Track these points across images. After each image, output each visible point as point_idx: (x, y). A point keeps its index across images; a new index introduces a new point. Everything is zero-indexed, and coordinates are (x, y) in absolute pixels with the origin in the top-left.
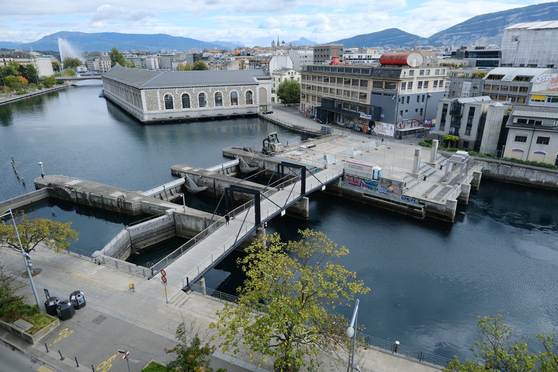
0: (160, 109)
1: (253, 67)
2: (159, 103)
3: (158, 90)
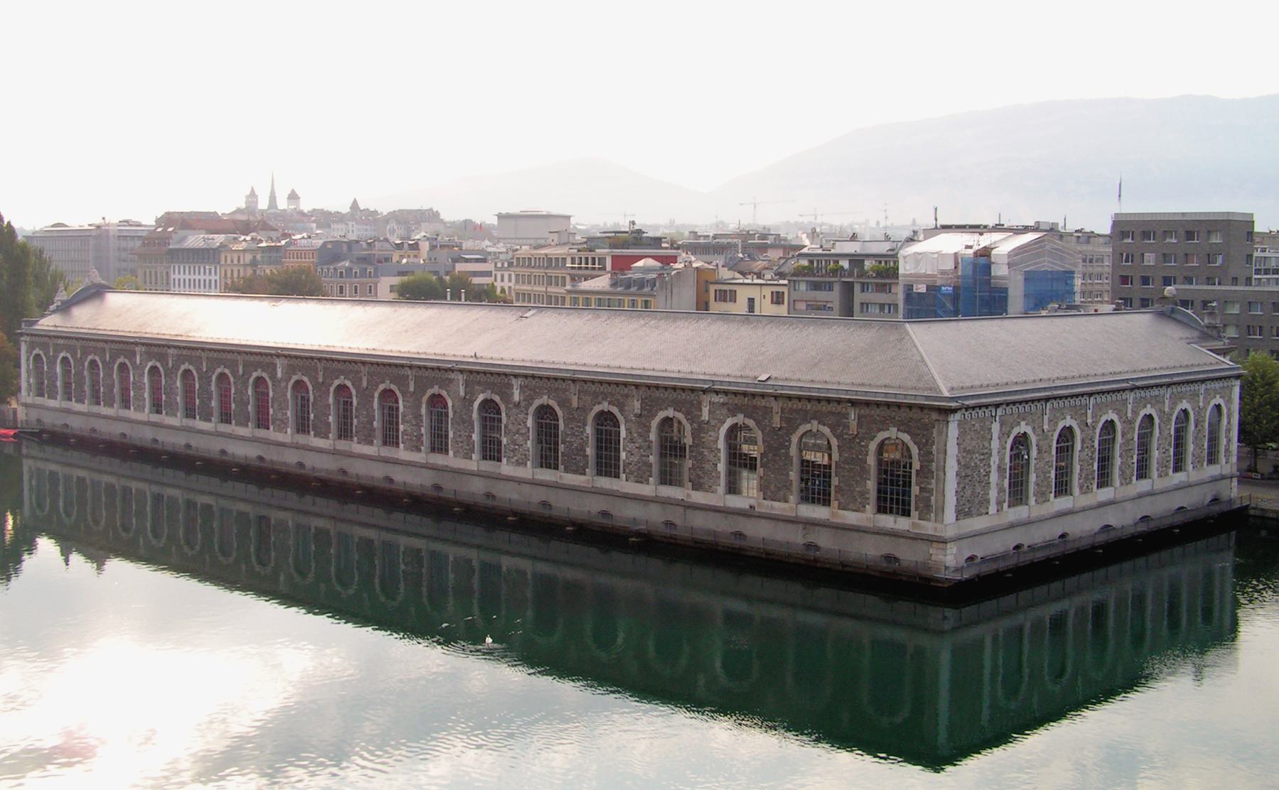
0: (992, 509)
1: (833, 297)
2: (994, 477)
3: (1000, 411)
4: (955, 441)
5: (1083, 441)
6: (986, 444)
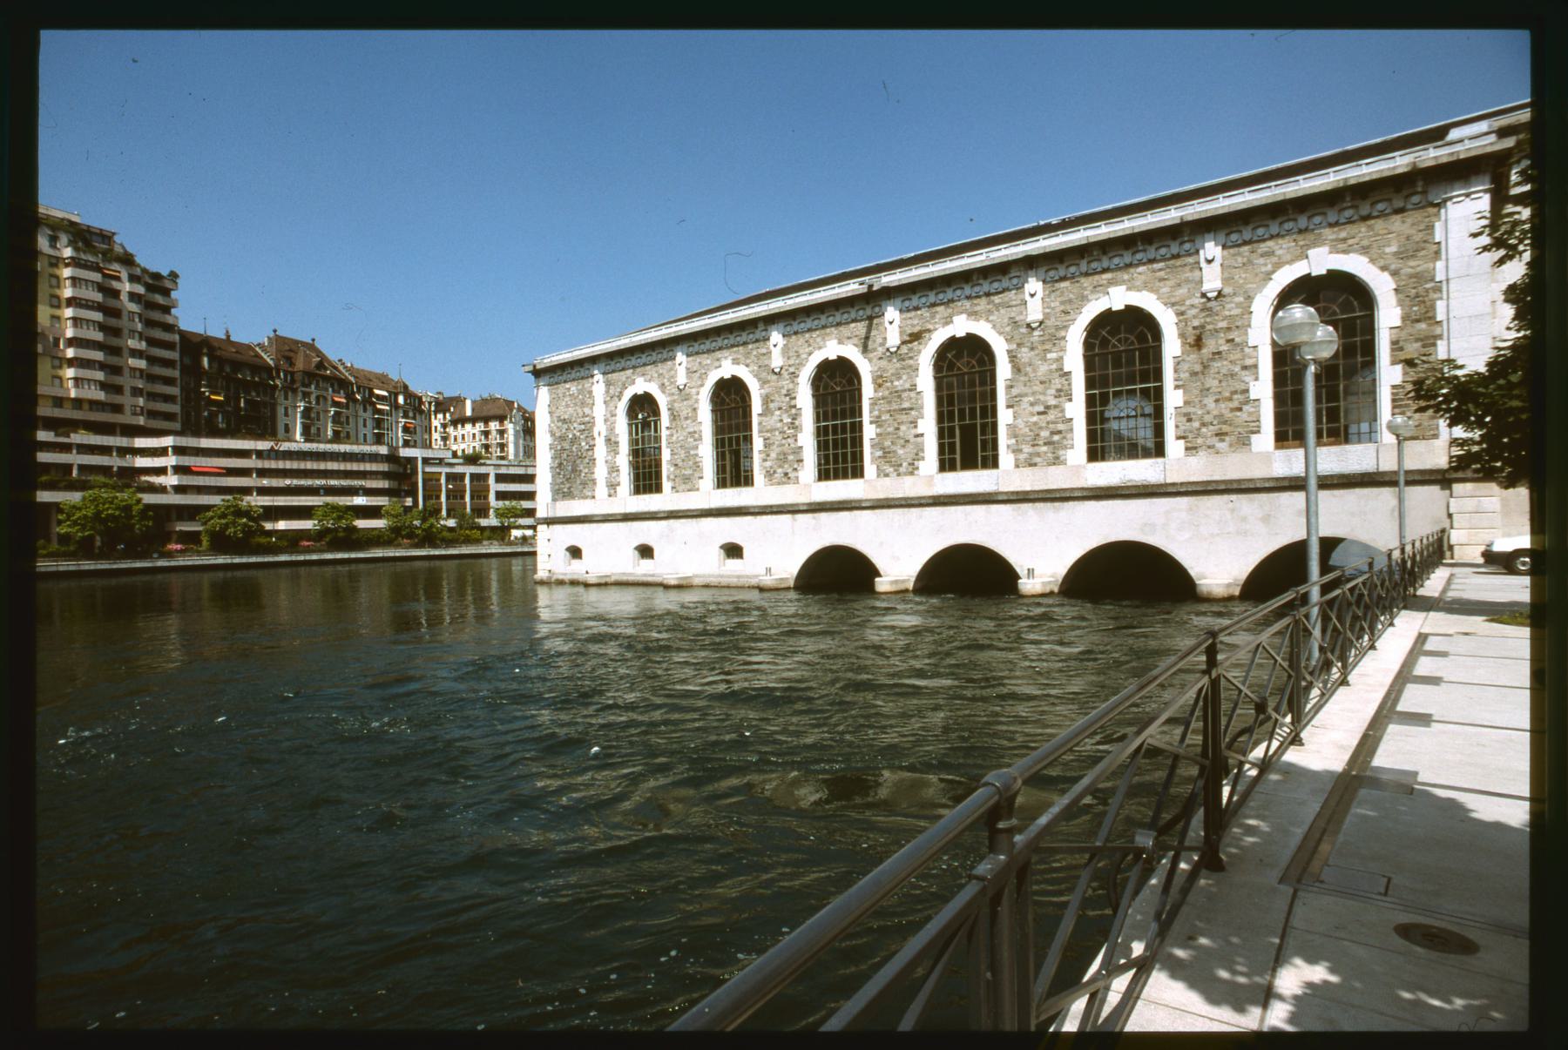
4: (547, 410)
5: (767, 400)
6: (587, 411)
